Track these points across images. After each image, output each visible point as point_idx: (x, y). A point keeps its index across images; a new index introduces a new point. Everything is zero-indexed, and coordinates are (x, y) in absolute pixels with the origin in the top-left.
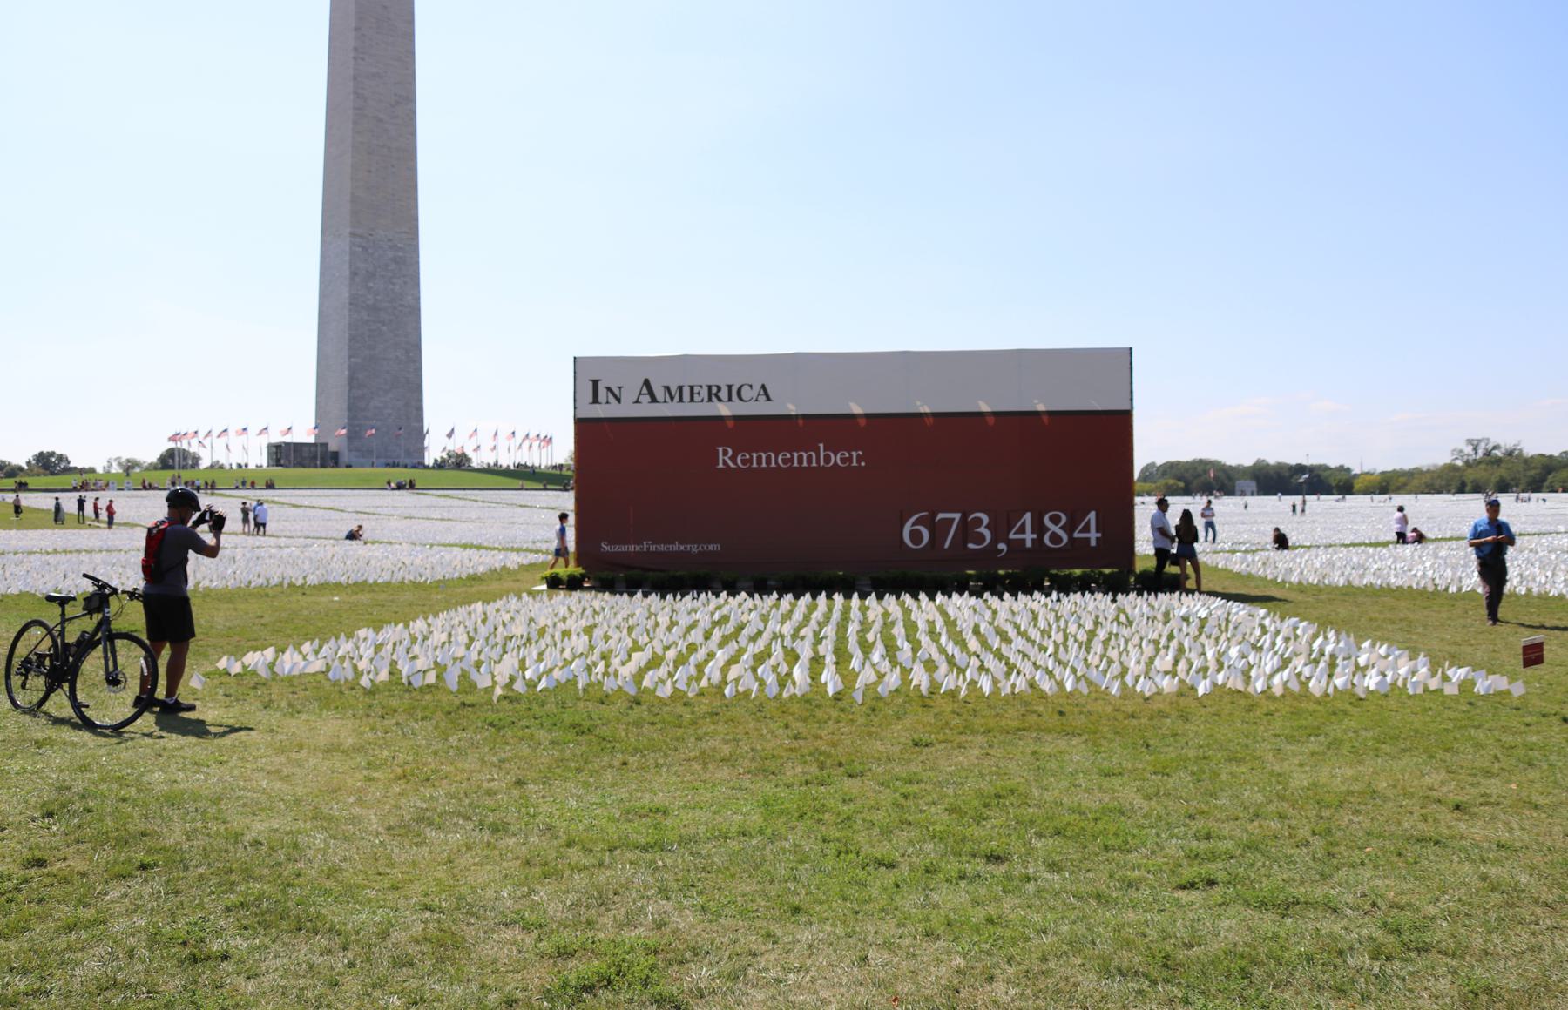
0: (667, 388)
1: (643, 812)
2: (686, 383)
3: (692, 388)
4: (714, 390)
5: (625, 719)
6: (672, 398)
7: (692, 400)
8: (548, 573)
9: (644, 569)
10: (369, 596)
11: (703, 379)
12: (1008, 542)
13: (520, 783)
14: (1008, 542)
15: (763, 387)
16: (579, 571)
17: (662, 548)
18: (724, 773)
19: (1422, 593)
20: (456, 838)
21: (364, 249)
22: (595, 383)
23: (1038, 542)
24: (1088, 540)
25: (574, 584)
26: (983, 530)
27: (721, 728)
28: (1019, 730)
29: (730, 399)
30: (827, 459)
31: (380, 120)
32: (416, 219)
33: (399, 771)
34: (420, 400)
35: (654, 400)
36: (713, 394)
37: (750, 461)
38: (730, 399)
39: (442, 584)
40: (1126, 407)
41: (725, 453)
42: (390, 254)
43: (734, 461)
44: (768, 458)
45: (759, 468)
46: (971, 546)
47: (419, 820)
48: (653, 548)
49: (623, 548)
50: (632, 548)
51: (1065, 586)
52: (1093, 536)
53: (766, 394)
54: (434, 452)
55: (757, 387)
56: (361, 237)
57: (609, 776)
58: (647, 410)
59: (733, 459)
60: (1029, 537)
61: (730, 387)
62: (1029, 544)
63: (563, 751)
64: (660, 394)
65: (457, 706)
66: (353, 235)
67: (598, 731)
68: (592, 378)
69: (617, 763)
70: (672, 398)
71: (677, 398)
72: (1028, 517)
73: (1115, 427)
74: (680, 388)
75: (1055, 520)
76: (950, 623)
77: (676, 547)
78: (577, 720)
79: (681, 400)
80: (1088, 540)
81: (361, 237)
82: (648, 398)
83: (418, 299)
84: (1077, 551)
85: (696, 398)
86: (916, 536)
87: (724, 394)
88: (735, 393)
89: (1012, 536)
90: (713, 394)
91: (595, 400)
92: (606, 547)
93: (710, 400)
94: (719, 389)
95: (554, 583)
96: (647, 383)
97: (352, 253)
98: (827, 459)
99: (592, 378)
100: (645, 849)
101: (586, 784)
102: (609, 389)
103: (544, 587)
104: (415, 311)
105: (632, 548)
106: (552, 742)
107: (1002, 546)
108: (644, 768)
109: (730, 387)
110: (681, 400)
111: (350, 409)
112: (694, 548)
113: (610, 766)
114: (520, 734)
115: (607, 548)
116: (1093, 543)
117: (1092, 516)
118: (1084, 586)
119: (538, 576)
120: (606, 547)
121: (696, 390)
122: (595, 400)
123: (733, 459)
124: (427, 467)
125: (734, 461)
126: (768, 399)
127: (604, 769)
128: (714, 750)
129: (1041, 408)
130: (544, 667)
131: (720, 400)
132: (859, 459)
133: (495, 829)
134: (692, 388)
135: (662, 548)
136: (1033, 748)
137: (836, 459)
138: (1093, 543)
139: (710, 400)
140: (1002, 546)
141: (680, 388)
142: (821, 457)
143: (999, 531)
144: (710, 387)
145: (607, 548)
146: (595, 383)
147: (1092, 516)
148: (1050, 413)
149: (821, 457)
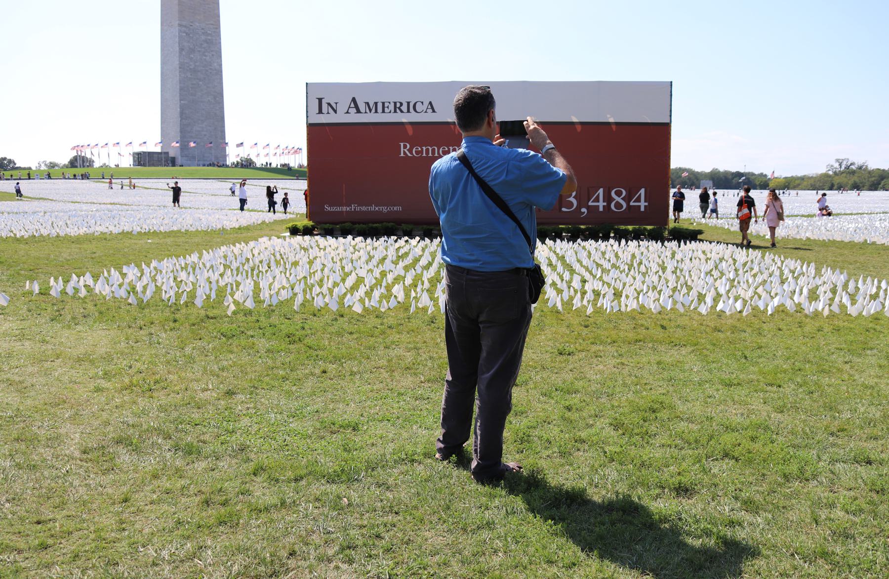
0: (367, 104)
1: (335, 428)
2: (380, 100)
3: (383, 103)
4: (398, 105)
5: (331, 329)
6: (370, 111)
7: (383, 111)
8: (290, 225)
9: (354, 223)
10: (172, 239)
11: (391, 98)
12: (588, 208)
13: (230, 393)
14: (588, 208)
15: (430, 103)
16: (311, 223)
17: (364, 208)
18: (408, 381)
19: (851, 245)
20: (150, 463)
22: (320, 100)
23: (607, 208)
24: (639, 206)
26: (572, 199)
27: (405, 337)
28: (636, 341)
29: (408, 111)
33: (127, 380)
35: (358, 111)
36: (397, 107)
37: (422, 152)
38: (408, 111)
39: (223, 231)
40: (668, 121)
41: (405, 147)
42: (203, 37)
43: (411, 153)
44: (433, 151)
45: (427, 157)
46: (564, 209)
47: (119, 442)
48: (358, 209)
49: (339, 209)
50: (344, 209)
51: (621, 236)
52: (643, 204)
53: (432, 108)
54: (233, 155)
55: (426, 103)
56: (185, 26)
57: (309, 384)
59: (410, 151)
60: (601, 204)
61: (408, 103)
62: (601, 209)
63: (274, 360)
64: (362, 107)
65: (200, 321)
66: (180, 25)
67: (307, 341)
68: (318, 98)
69: (317, 371)
70: (370, 111)
71: (373, 110)
72: (601, 191)
73: (658, 135)
74: (376, 104)
75: (619, 194)
76: (562, 259)
77: (373, 208)
78: (292, 330)
79: (376, 112)
80: (639, 206)
81: (185, 26)
82: (354, 110)
83: (221, 65)
84: (633, 215)
85: (386, 110)
87: (404, 108)
88: (412, 107)
89: (590, 204)
90: (397, 107)
91: (320, 112)
92: (327, 208)
93: (395, 111)
94: (401, 104)
95: (294, 231)
96: (354, 100)
97: (180, 37)
99: (318, 98)
100: (331, 480)
101: (289, 394)
102: (329, 104)
104: (219, 72)
105: (344, 209)
106: (268, 351)
107: (584, 210)
108: (341, 376)
109: (408, 103)
110: (376, 112)
111: (181, 132)
112: (384, 209)
113: (312, 374)
114: (243, 343)
115: (329, 209)
116: (642, 209)
117: (642, 191)
118: (637, 236)
119: (284, 227)
120: (327, 208)
121: (386, 105)
122: (320, 112)
123: (410, 151)
124: (227, 166)
125: (411, 153)
126: (434, 111)
127: (306, 376)
128: (400, 358)
129: (611, 120)
130: (275, 286)
131: (402, 111)
133: (190, 451)
134: (383, 103)
135: (364, 208)
136: (654, 358)
138: (642, 209)
139: (395, 111)
140: (584, 210)
141: (376, 104)
143: (583, 200)
144: (395, 103)
145: (329, 209)
146: (320, 100)
147: (642, 191)
148: (617, 124)
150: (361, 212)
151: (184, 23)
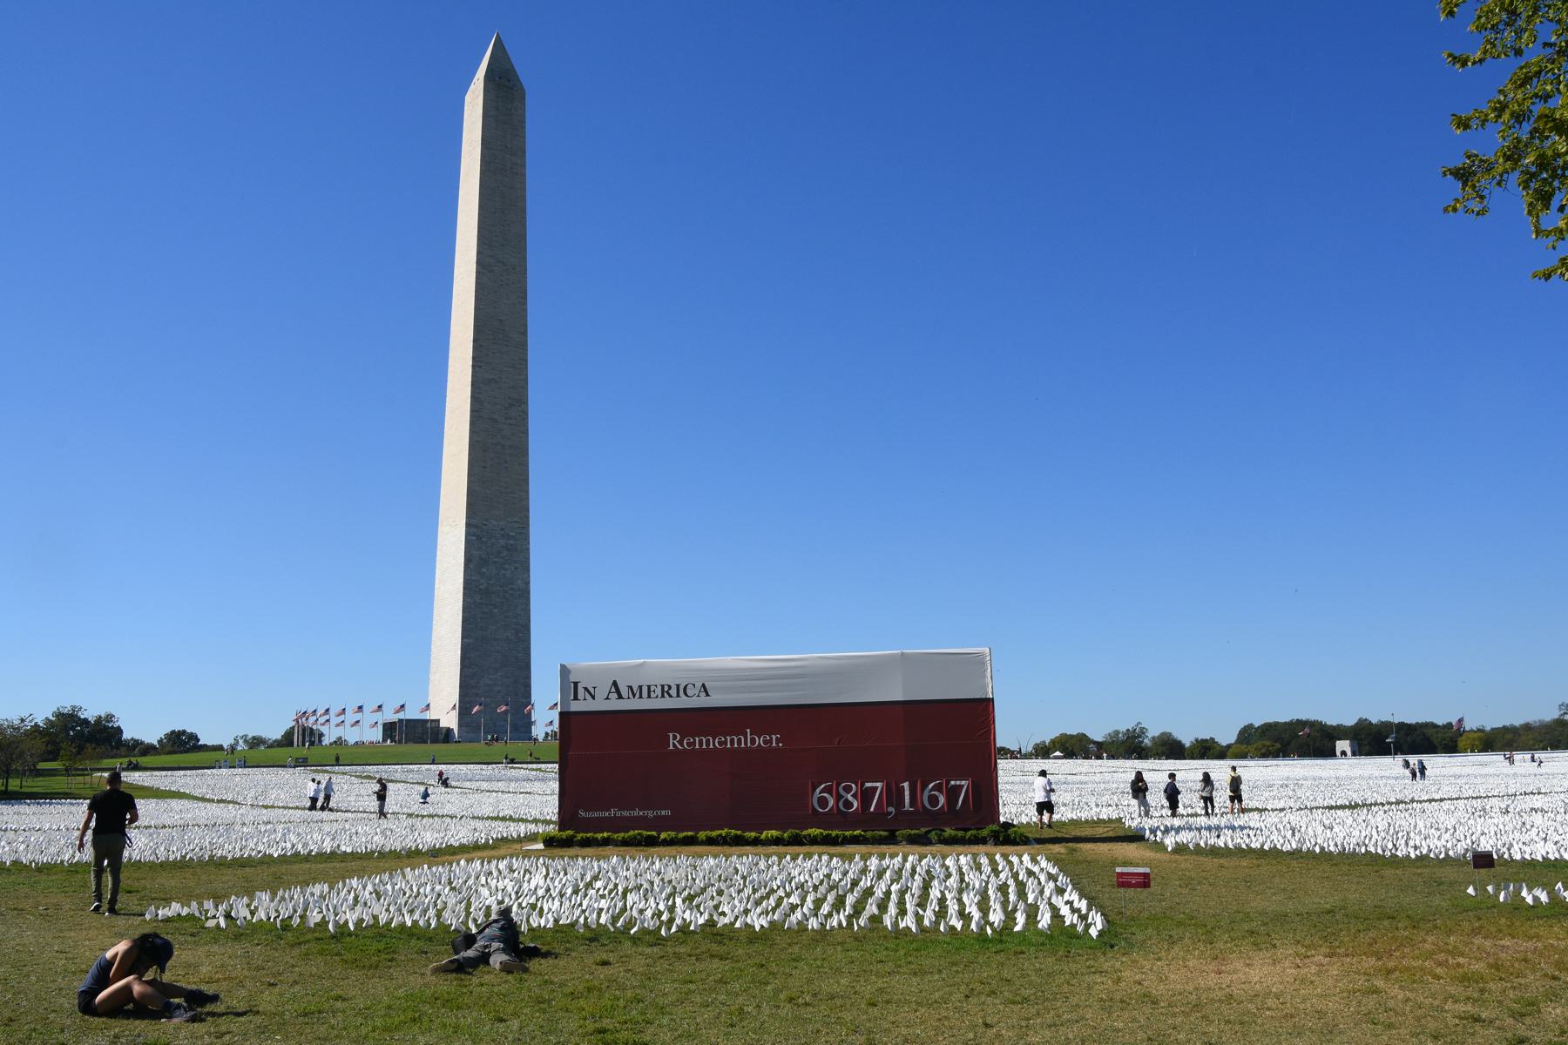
2: (645, 683)
11: (657, 680)
17: (626, 813)
21: (479, 538)
25: (566, 843)
30: (753, 741)
31: (495, 421)
32: (528, 510)
34: (529, 677)
35: (620, 697)
42: (502, 542)
48: (619, 814)
49: (596, 815)
58: (615, 705)
59: (681, 742)
64: (624, 692)
73: (979, 712)
77: (636, 813)
84: (951, 815)
86: (823, 802)
87: (673, 692)
90: (665, 691)
91: (576, 698)
96: (615, 683)
98: (753, 741)
103: (541, 846)
104: (525, 594)
123: (681, 742)
132: (778, 741)
135: (626, 813)
137: (759, 741)
142: (750, 740)
146: (576, 684)
149: (750, 740)
150: (623, 818)
151: (474, 521)
